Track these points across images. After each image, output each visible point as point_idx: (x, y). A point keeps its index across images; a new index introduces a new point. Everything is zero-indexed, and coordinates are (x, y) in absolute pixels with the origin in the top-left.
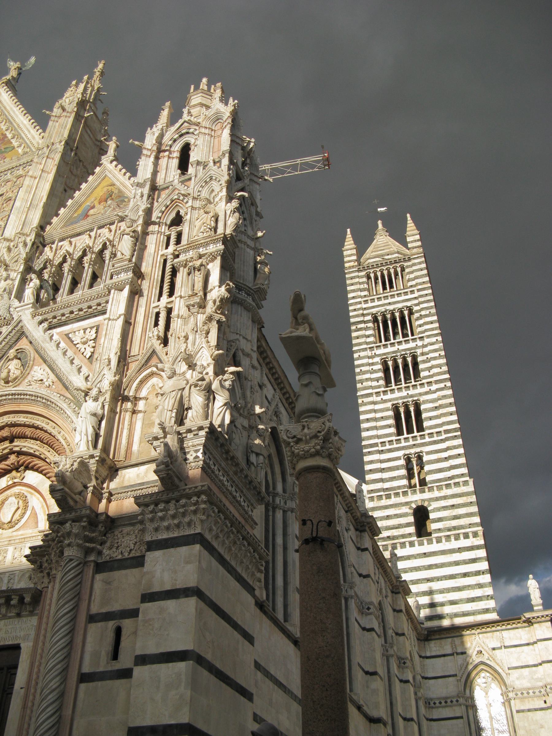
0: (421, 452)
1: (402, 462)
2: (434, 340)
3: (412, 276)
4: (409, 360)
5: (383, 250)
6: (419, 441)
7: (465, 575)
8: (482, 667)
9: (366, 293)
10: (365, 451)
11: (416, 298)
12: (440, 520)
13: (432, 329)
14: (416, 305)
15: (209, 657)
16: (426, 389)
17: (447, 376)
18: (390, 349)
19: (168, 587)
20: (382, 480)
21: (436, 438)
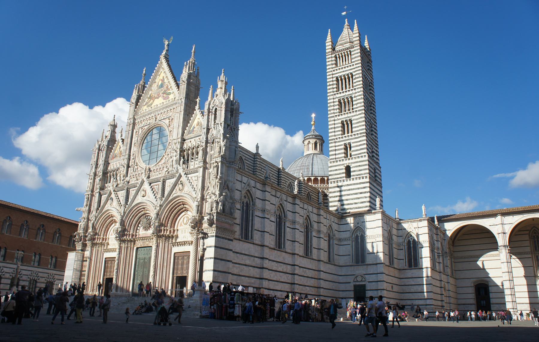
0: (351, 142)
1: (343, 147)
2: (359, 90)
4: (350, 99)
6: (350, 137)
7: (361, 193)
8: (358, 228)
10: (330, 142)
11: (354, 68)
12: (354, 171)
13: (360, 85)
14: (354, 72)
15: (218, 257)
16: (355, 114)
17: (363, 108)
18: (342, 95)
21: (356, 136)
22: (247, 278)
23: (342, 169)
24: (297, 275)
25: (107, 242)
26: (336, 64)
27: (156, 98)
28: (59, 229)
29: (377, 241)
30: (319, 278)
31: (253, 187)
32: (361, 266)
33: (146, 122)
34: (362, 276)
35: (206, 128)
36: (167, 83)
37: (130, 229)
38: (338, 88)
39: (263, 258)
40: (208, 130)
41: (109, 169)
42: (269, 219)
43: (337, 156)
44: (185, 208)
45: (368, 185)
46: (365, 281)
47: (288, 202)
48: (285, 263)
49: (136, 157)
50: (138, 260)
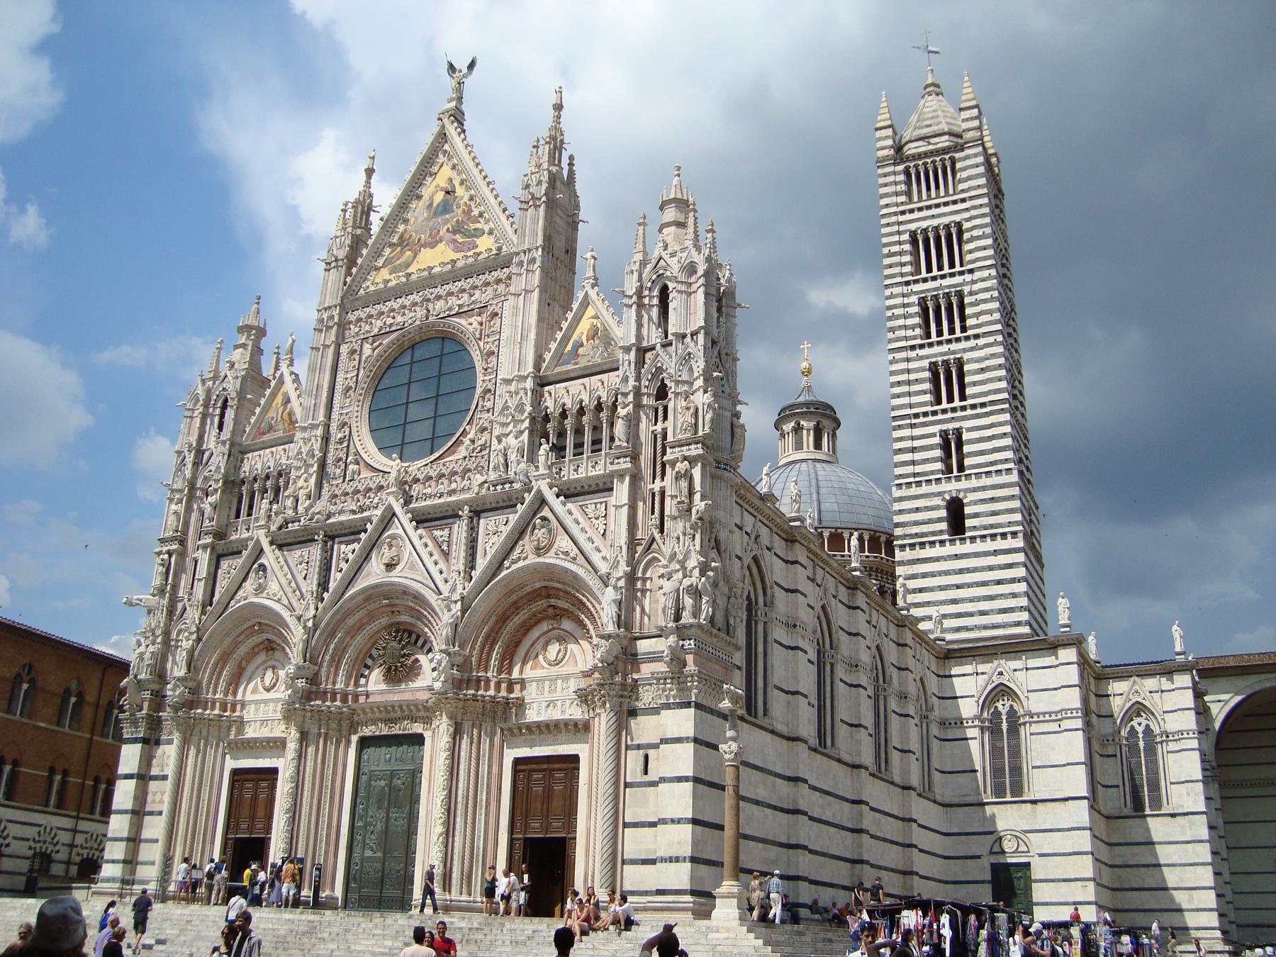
0: (961, 428)
1: (937, 440)
2: (985, 273)
3: (964, 175)
4: (954, 300)
5: (930, 126)
7: (999, 582)
8: (1001, 688)
9: (903, 199)
11: (967, 210)
12: (976, 515)
13: (985, 258)
14: (968, 220)
15: (703, 776)
16: (972, 343)
19: (676, 736)
20: (913, 463)
22: (760, 845)
23: (937, 508)
24: (867, 832)
25: (237, 714)
26: (909, 194)
27: (425, 246)
28: (31, 667)
29: (1066, 730)
30: (908, 842)
31: (768, 548)
32: (1014, 806)
33: (389, 321)
34: (1016, 837)
35: (634, 349)
36: (466, 199)
37: (336, 674)
38: (916, 264)
39: (795, 779)
40: (642, 352)
41: (246, 467)
42: (806, 652)
43: (918, 469)
44: (554, 607)
45: (1020, 557)
46: (1029, 852)
47: (840, 601)
48: (837, 797)
49: (355, 435)
50: (364, 778)
